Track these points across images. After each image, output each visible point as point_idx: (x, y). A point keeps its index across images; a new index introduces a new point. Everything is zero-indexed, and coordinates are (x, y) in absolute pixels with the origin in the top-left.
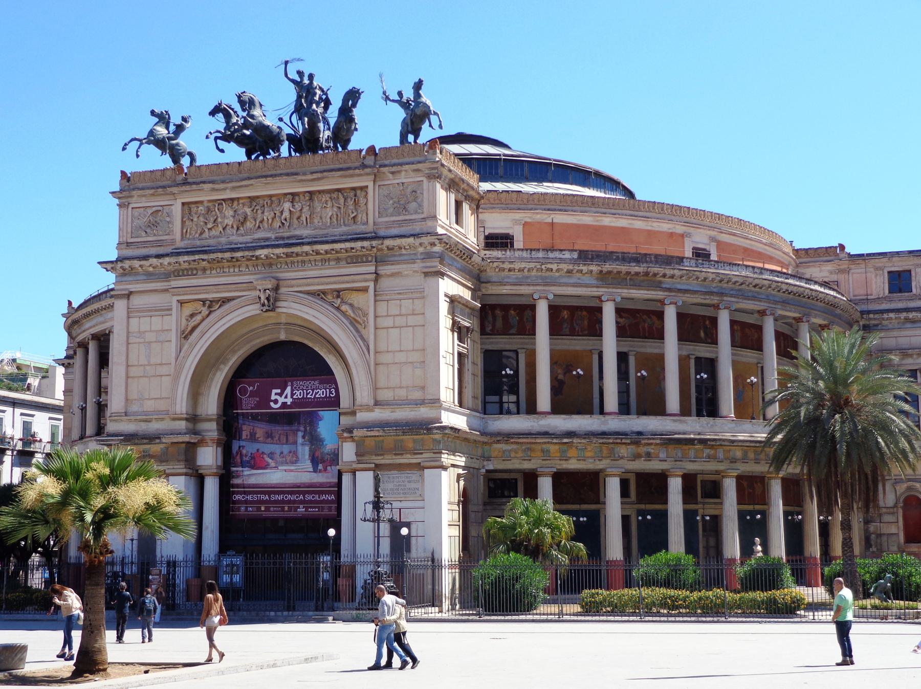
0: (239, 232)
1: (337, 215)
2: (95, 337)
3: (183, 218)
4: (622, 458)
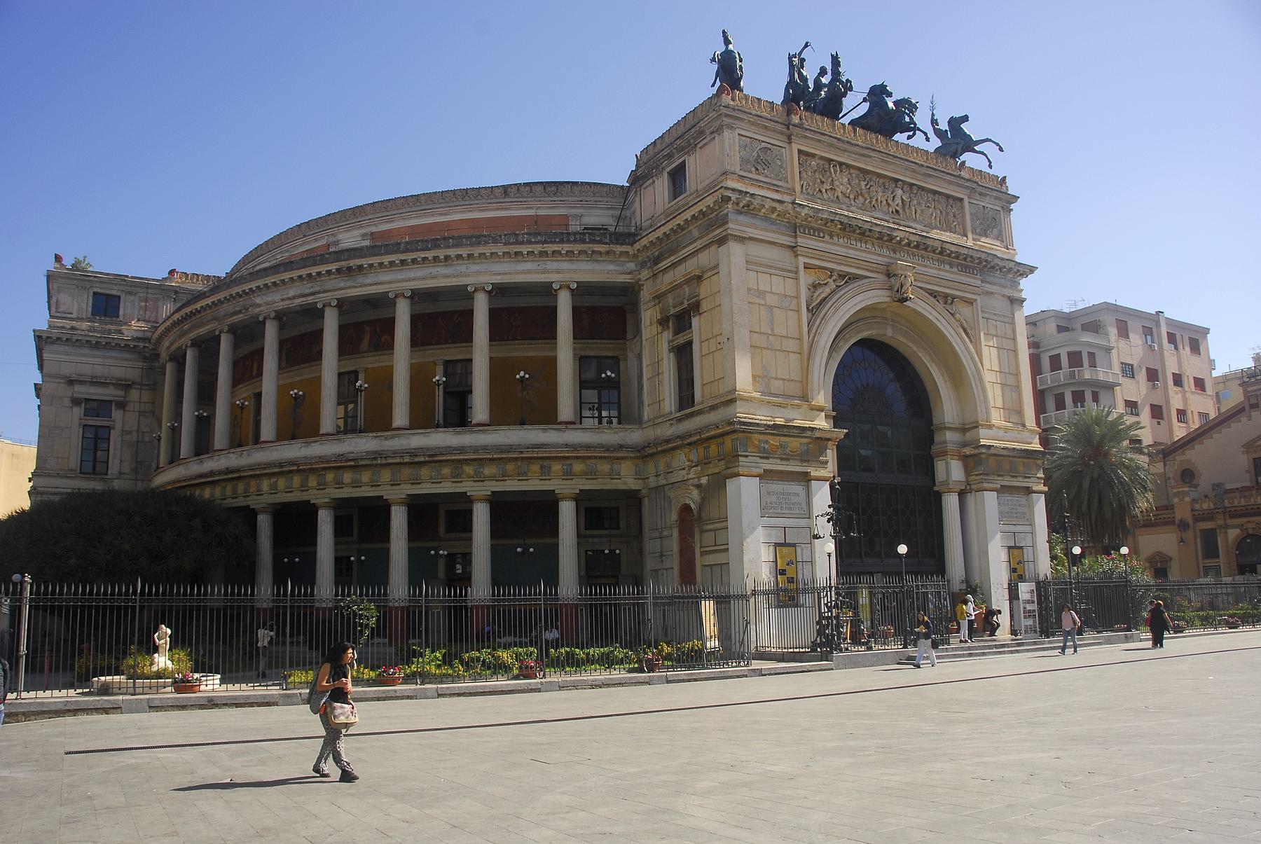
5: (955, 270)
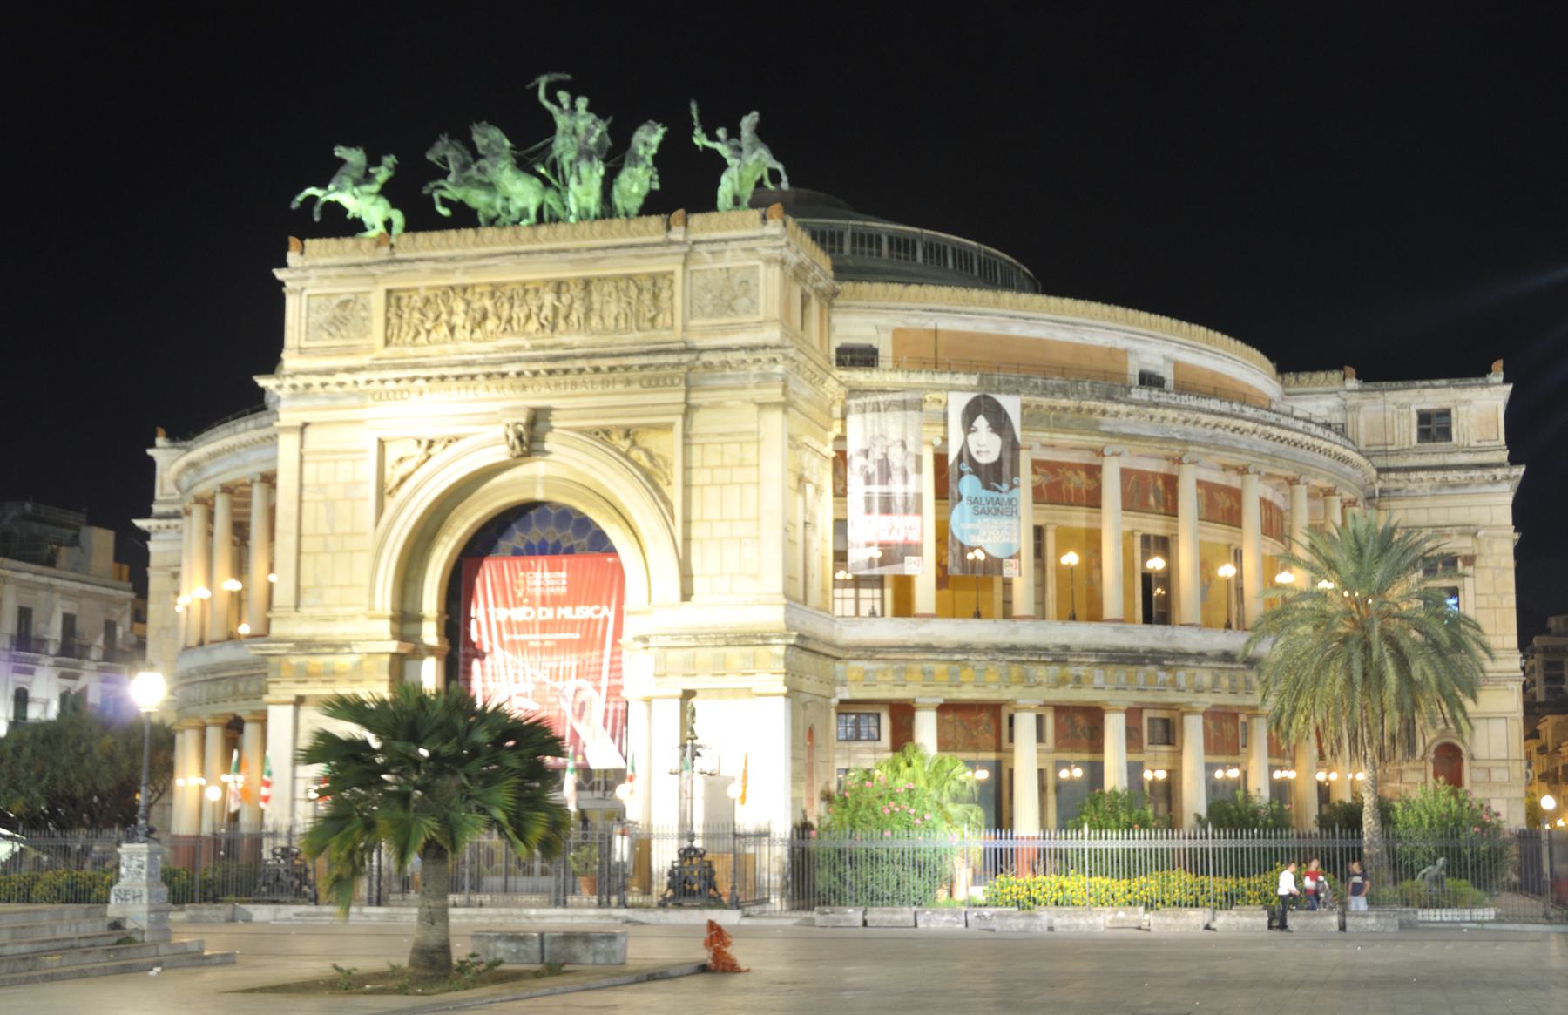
0: (474, 336)
1: (626, 315)
2: (227, 489)
3: (387, 311)
4: (1039, 684)
5: (636, 387)
